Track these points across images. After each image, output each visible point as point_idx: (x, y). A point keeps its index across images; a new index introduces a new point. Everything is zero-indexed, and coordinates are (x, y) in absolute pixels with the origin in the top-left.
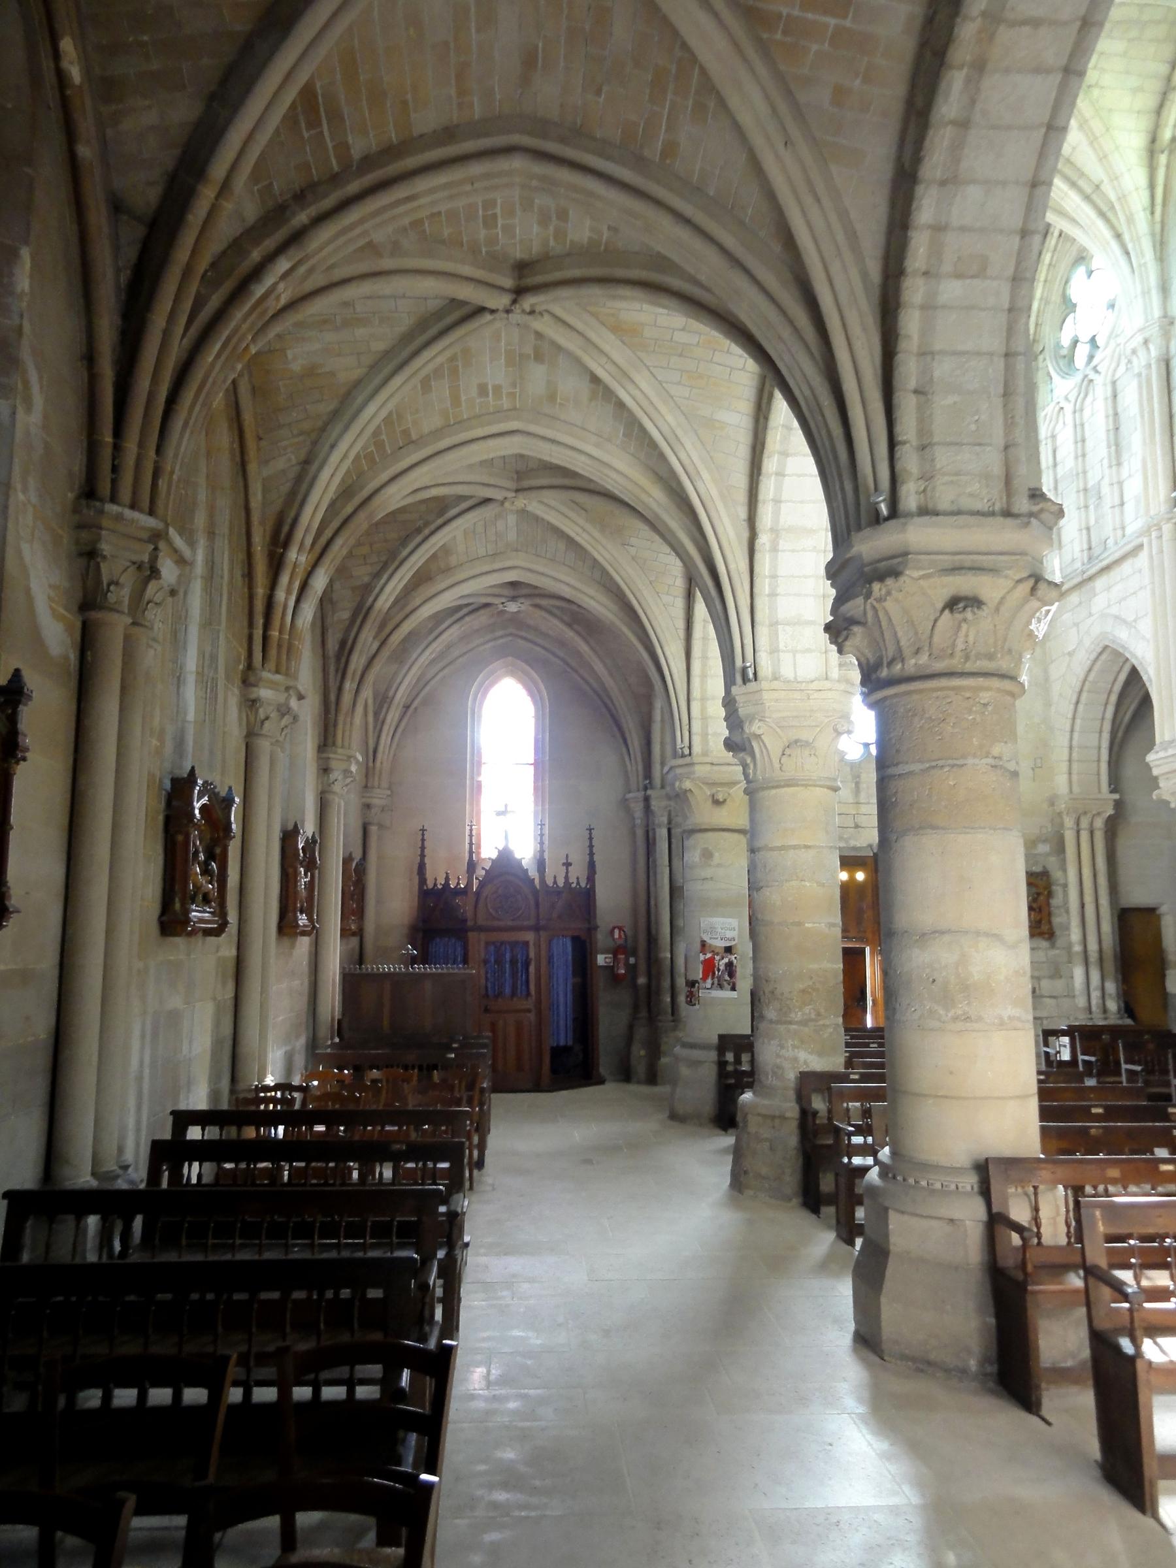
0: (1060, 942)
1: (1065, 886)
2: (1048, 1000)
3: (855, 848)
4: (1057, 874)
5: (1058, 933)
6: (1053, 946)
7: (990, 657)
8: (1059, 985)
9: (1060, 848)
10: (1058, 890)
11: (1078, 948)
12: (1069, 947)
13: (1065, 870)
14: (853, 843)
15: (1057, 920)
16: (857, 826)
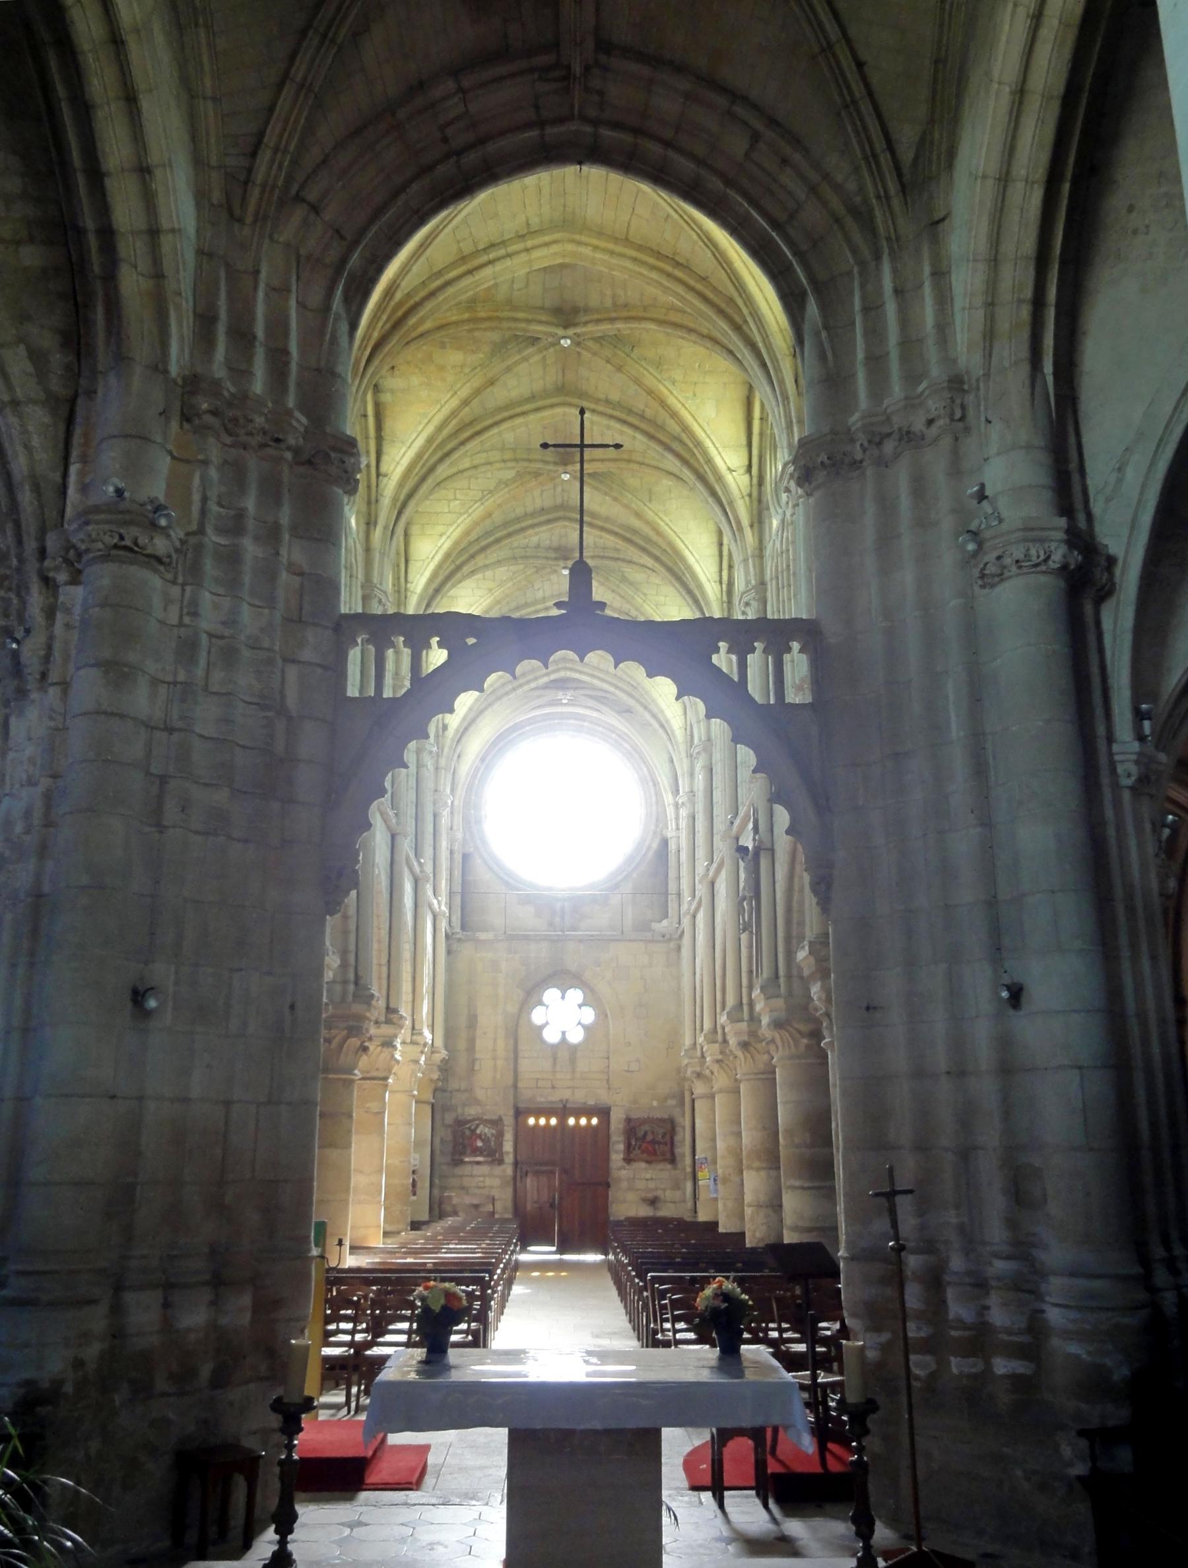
0: (679, 1166)
1: (684, 1128)
2: (670, 1204)
3: (552, 1102)
4: (679, 1119)
5: (678, 1159)
6: (675, 1169)
7: (368, 1072)
8: (677, 1195)
9: (682, 1103)
10: (678, 1129)
11: (689, 1170)
12: (684, 1169)
13: (683, 1115)
14: (551, 1099)
15: (678, 1151)
16: (553, 1087)
